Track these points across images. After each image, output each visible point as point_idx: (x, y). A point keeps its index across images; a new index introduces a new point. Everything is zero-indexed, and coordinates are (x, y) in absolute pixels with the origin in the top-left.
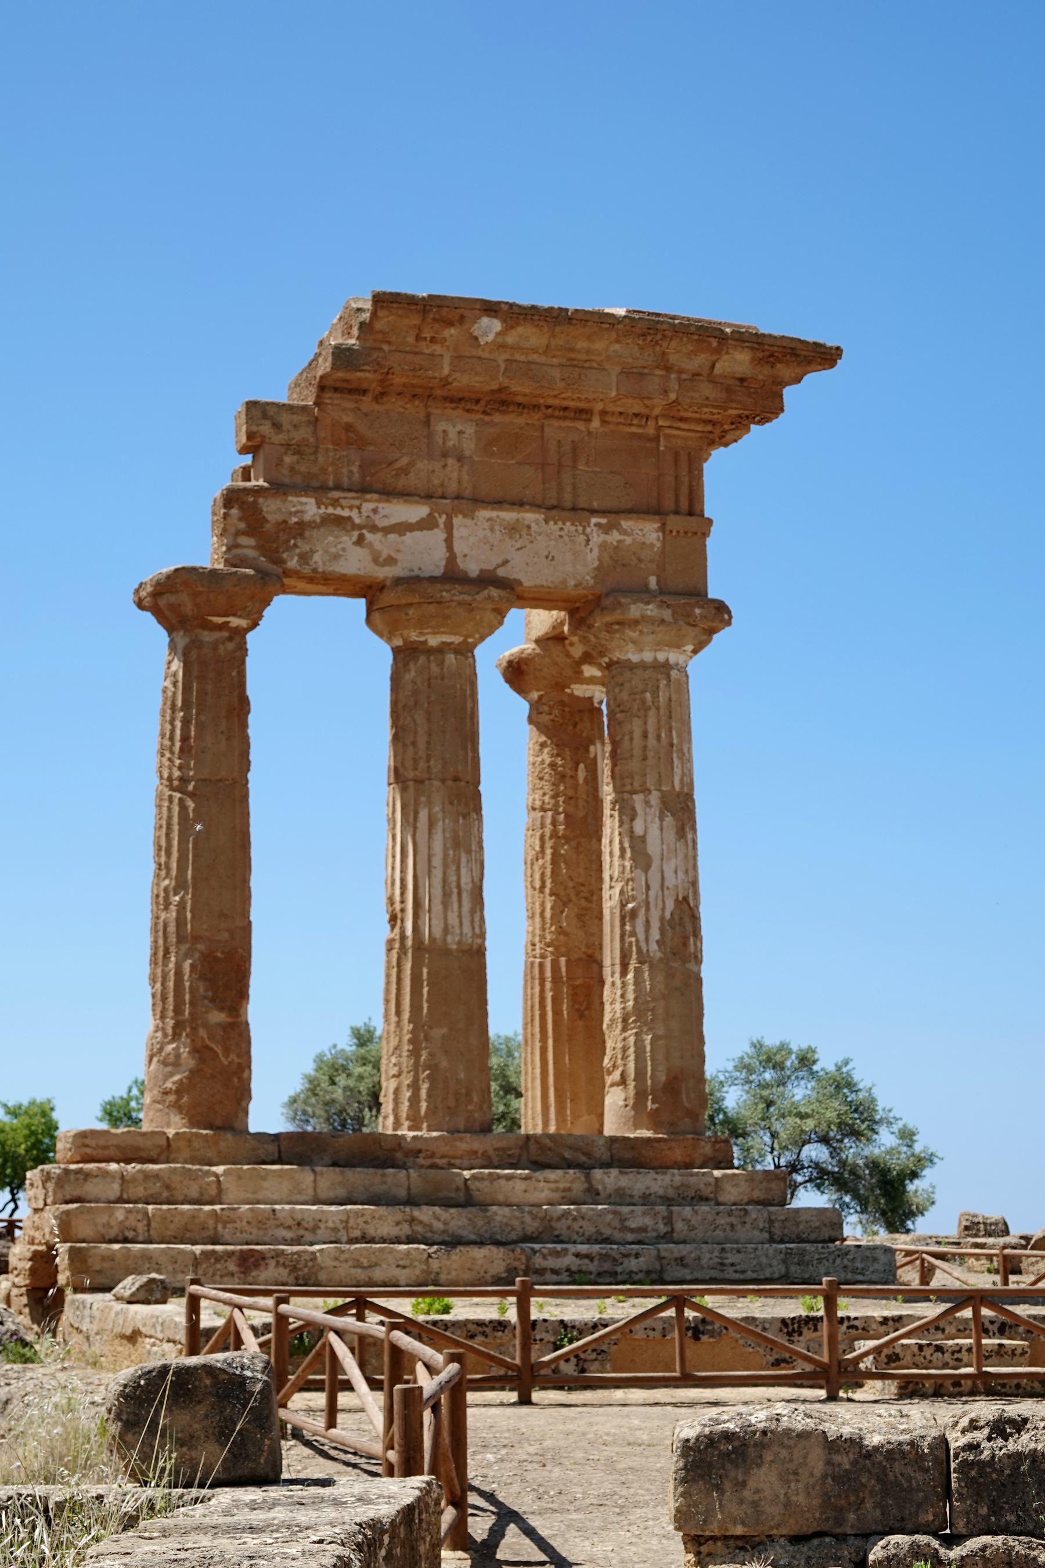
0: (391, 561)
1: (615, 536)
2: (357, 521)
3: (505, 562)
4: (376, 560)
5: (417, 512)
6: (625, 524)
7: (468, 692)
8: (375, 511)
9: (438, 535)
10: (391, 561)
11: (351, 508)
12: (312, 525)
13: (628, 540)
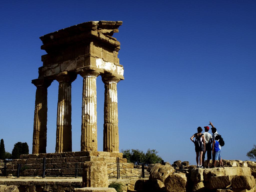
0: (54, 72)
2: (51, 68)
4: (53, 73)
5: (56, 65)
7: (64, 88)
8: (53, 66)
9: (59, 67)
10: (54, 72)
11: (50, 66)
12: (46, 70)
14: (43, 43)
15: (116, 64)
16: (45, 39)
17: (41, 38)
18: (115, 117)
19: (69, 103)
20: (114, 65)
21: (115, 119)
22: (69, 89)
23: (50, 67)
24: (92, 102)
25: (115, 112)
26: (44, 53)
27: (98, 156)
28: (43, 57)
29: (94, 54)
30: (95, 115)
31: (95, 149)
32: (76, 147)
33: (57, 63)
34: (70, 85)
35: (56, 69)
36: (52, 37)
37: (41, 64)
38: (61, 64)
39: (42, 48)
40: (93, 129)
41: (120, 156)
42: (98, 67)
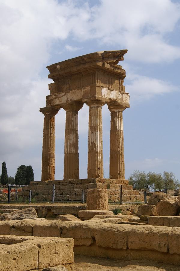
0: (61, 101)
1: (85, 89)
3: (73, 97)
5: (63, 94)
6: (86, 88)
9: (66, 96)
10: (61, 101)
12: (54, 99)
13: (86, 90)
14: (50, 72)
15: (122, 91)
16: (52, 68)
17: (48, 67)
18: (121, 145)
19: (76, 131)
20: (120, 93)
21: (121, 147)
22: (75, 117)
23: (57, 96)
24: (97, 131)
25: (121, 140)
26: (52, 81)
27: (104, 183)
28: (49, 85)
29: (99, 83)
30: (101, 144)
31: (101, 176)
32: (83, 174)
33: (64, 92)
34: (76, 113)
35: (64, 98)
36: (58, 67)
37: (48, 93)
38: (68, 93)
39: (49, 77)
40: (99, 157)
41: (126, 183)
42: (103, 96)
